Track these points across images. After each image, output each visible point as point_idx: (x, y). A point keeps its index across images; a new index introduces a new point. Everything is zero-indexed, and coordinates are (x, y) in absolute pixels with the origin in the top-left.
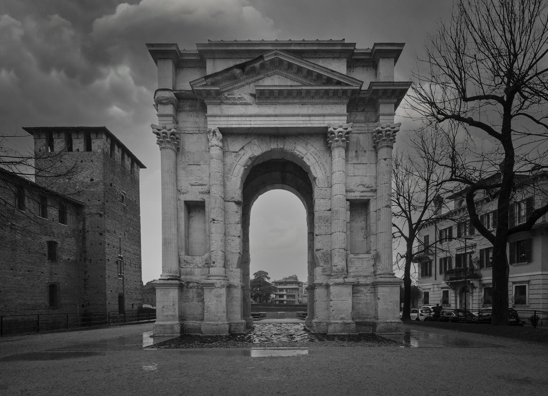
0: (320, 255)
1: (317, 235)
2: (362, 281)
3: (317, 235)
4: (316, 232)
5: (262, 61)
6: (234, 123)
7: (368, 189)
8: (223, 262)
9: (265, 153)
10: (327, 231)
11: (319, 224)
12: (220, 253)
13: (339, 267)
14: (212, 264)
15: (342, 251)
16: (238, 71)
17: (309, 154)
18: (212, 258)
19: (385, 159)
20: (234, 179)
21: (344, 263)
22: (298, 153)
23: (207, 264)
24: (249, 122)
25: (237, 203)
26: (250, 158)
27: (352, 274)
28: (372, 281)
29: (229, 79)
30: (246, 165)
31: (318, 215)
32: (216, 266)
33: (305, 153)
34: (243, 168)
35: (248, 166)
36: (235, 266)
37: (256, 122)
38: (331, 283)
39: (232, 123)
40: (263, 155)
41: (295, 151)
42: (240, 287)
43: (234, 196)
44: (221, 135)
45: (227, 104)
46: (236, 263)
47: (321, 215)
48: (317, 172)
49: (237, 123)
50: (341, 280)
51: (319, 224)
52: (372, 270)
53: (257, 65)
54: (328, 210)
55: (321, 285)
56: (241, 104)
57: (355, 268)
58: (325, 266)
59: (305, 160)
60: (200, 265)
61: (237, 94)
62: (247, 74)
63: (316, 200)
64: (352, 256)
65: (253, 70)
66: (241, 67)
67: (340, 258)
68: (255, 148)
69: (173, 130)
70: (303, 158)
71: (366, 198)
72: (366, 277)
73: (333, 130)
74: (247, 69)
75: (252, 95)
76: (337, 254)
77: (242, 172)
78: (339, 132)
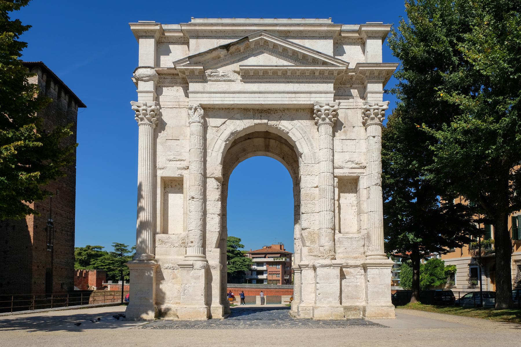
0: (307, 234)
1: (303, 213)
2: (351, 262)
3: (303, 213)
4: (303, 209)
6: (217, 99)
9: (248, 128)
10: (313, 209)
11: (305, 202)
13: (327, 248)
14: (190, 244)
15: (330, 231)
17: (294, 129)
18: (189, 237)
19: (374, 137)
20: (214, 154)
21: (331, 243)
23: (184, 243)
24: (231, 99)
27: (341, 255)
28: (362, 262)
30: (228, 140)
31: (304, 192)
32: (194, 246)
34: (224, 143)
36: (214, 246)
37: (239, 99)
38: (318, 265)
39: (214, 99)
41: (280, 126)
43: (215, 172)
44: (203, 111)
45: (210, 81)
47: (308, 192)
48: (302, 147)
49: (220, 99)
50: (328, 262)
51: (305, 202)
52: (362, 250)
54: (315, 187)
55: (307, 266)
56: (225, 81)
57: (344, 248)
58: (312, 246)
59: (290, 135)
60: (176, 245)
61: (221, 71)
63: (302, 176)
67: (327, 238)
68: (238, 122)
69: (153, 107)
72: (355, 258)
73: (320, 108)
75: (235, 72)
76: (324, 234)
77: (223, 147)
78: (325, 110)
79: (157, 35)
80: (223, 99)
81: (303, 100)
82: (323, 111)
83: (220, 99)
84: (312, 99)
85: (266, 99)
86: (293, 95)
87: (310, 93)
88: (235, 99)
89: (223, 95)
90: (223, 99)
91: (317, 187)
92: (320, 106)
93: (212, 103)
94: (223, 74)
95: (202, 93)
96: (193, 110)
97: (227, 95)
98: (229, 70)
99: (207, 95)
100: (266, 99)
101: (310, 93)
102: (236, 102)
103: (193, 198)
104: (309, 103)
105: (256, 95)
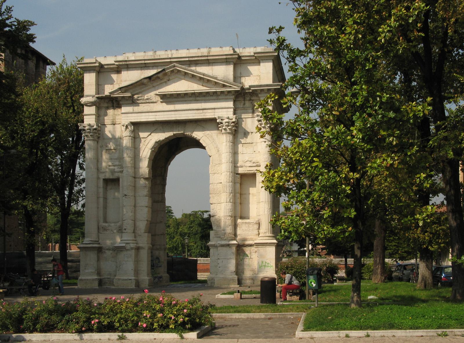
5: (164, 72)
7: (254, 165)
8: (133, 229)
12: (131, 222)
16: (146, 81)
22: (195, 137)
25: (146, 179)
26: (156, 142)
29: (139, 85)
33: (201, 136)
34: (150, 151)
35: (155, 148)
40: (166, 138)
42: (147, 248)
46: (144, 228)
53: (160, 75)
56: (149, 103)
62: (153, 80)
64: (239, 221)
65: (158, 78)
66: (150, 78)
68: (160, 134)
70: (200, 140)
71: (253, 172)
74: (153, 79)
79: (97, 69)
80: (147, 117)
81: (209, 115)
82: (224, 123)
83: (145, 117)
84: (216, 114)
85: (180, 116)
86: (201, 111)
87: (214, 109)
88: (157, 117)
89: (147, 114)
90: (147, 117)
91: (221, 183)
92: (222, 120)
93: (139, 120)
94: (147, 98)
95: (131, 113)
96: (125, 128)
97: (150, 114)
98: (152, 95)
99: (136, 115)
100: (180, 116)
101: (214, 109)
102: (157, 119)
103: (126, 195)
104: (213, 117)
105: (173, 113)
